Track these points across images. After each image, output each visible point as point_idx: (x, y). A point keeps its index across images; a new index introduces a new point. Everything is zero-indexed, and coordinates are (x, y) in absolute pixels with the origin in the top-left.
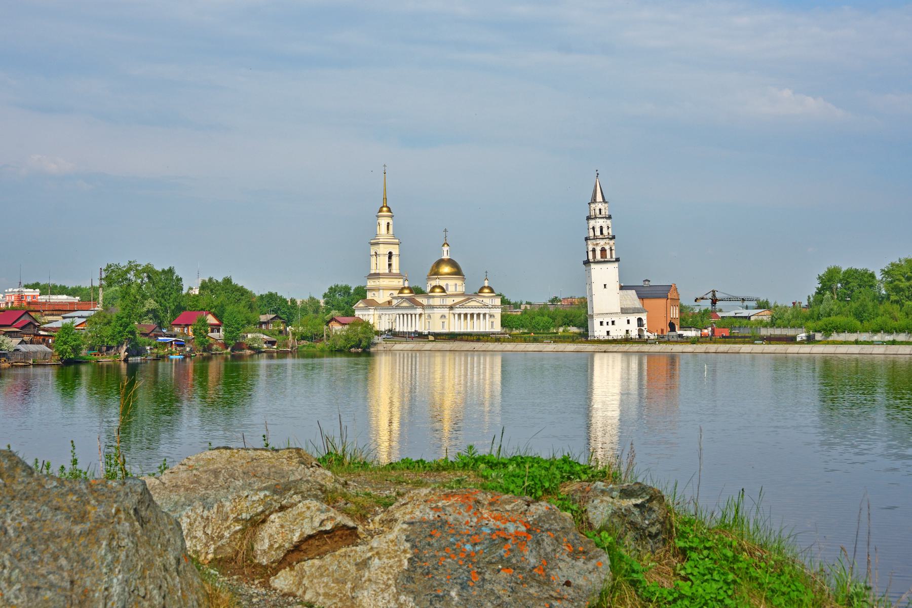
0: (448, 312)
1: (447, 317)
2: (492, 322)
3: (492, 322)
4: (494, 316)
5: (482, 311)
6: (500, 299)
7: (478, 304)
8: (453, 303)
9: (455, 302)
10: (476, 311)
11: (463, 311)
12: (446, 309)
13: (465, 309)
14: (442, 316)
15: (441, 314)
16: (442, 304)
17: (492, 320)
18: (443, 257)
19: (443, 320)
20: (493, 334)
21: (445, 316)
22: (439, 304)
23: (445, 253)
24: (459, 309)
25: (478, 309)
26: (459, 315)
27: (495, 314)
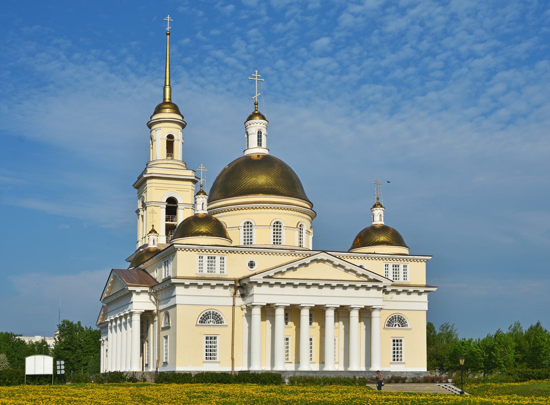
0: (230, 301)
1: (227, 319)
2: (397, 342)
3: (397, 342)
6: (424, 264)
7: (351, 277)
8: (247, 271)
9: (256, 269)
12: (219, 291)
14: (204, 319)
15: (199, 312)
16: (205, 272)
17: (397, 332)
18: (248, 152)
20: (397, 379)
21: (218, 319)
22: (194, 272)
23: (253, 139)
27: (406, 316)
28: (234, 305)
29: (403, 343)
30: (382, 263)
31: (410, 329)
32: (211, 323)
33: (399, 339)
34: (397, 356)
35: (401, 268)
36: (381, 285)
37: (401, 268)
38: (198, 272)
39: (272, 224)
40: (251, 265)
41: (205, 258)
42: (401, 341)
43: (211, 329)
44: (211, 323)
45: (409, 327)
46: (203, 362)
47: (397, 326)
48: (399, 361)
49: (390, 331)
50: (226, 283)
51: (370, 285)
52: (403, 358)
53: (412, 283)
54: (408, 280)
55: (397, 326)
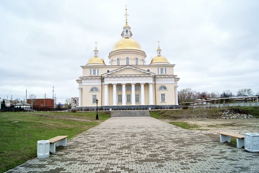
0: (100, 84)
2: (163, 95)
3: (163, 95)
4: (165, 88)
5: (142, 81)
10: (133, 81)
11: (115, 82)
12: (96, 81)
13: (117, 79)
14: (92, 90)
15: (91, 87)
17: (163, 92)
19: (94, 93)
22: (88, 75)
24: (108, 79)
25: (135, 79)
26: (110, 86)
27: (167, 86)
28: (102, 85)
29: (165, 95)
30: (157, 69)
31: (168, 90)
32: (94, 91)
33: (164, 94)
34: (163, 100)
35: (164, 69)
36: (151, 75)
37: (164, 69)
38: (90, 75)
39: (126, 58)
40: (108, 71)
41: (92, 70)
42: (164, 95)
43: (94, 93)
44: (94, 91)
45: (167, 90)
46: (92, 104)
47: (163, 90)
48: (164, 102)
49: (160, 91)
50: (98, 78)
51: (147, 75)
52: (165, 100)
53: (168, 74)
54: (167, 74)
55: (163, 90)
